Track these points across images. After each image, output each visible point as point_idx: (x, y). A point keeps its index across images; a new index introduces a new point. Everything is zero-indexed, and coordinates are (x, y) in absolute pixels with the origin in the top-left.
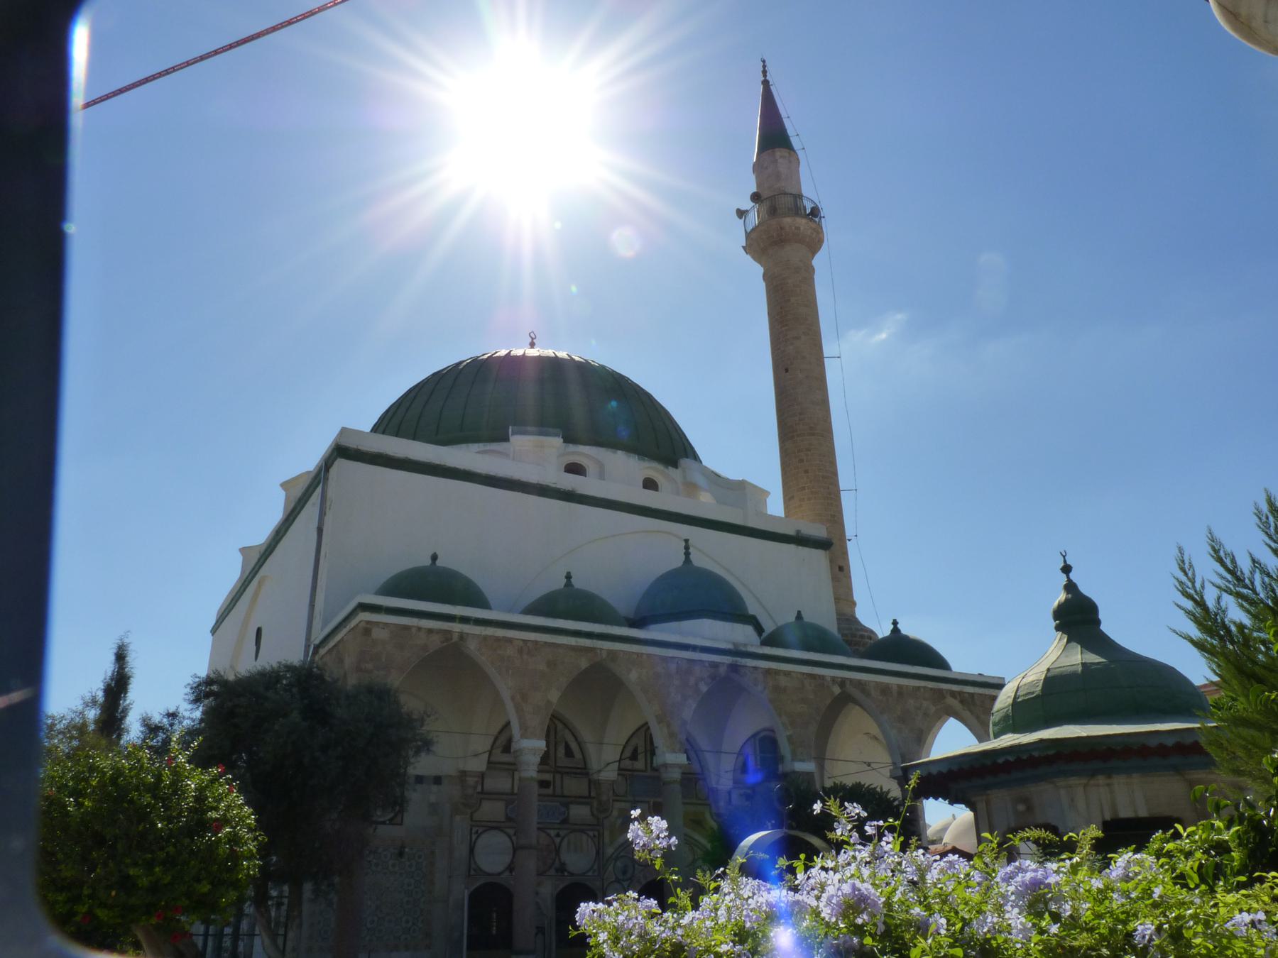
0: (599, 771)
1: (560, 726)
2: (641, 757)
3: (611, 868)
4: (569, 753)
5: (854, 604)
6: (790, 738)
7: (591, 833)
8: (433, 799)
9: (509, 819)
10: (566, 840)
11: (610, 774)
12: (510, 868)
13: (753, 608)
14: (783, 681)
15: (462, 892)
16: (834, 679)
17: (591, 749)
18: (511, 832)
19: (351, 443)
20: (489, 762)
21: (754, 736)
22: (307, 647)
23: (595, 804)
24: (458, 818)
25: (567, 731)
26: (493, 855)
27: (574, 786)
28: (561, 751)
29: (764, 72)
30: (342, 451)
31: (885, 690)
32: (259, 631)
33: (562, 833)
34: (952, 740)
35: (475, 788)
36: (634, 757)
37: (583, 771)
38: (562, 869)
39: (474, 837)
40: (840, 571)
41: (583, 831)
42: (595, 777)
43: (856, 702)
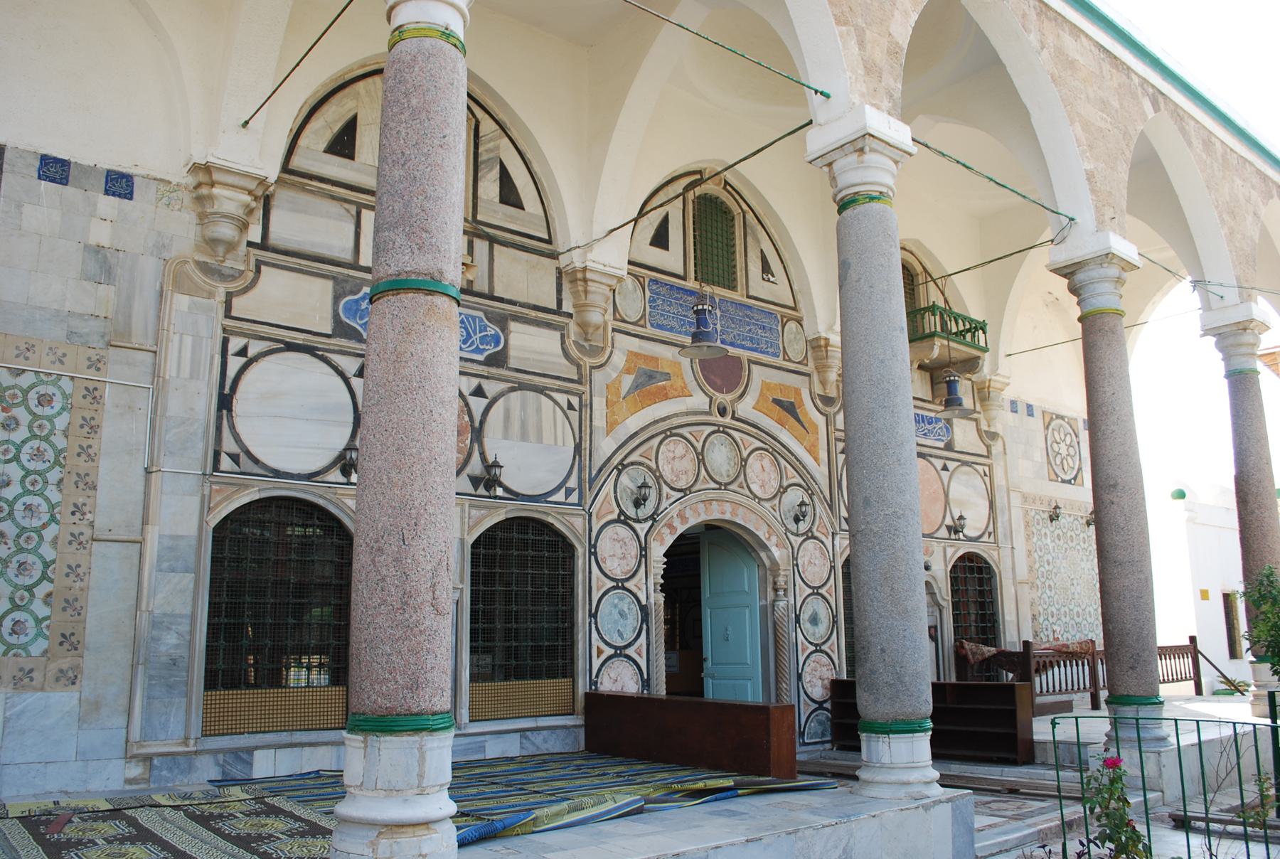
0: (589, 246)
3: (609, 486)
4: (509, 195)
6: (1090, 176)
7: (562, 399)
8: (100, 235)
9: (341, 329)
10: (500, 402)
12: (345, 464)
15: (184, 516)
16: (1144, 81)
18: (350, 365)
20: (285, 168)
23: (573, 327)
24: (182, 302)
25: (506, 139)
26: (293, 425)
27: (521, 278)
28: (490, 188)
31: (1208, 140)
33: (491, 388)
35: (244, 227)
36: (660, 239)
37: (543, 246)
38: (488, 480)
39: (234, 364)
41: (541, 390)
42: (576, 260)
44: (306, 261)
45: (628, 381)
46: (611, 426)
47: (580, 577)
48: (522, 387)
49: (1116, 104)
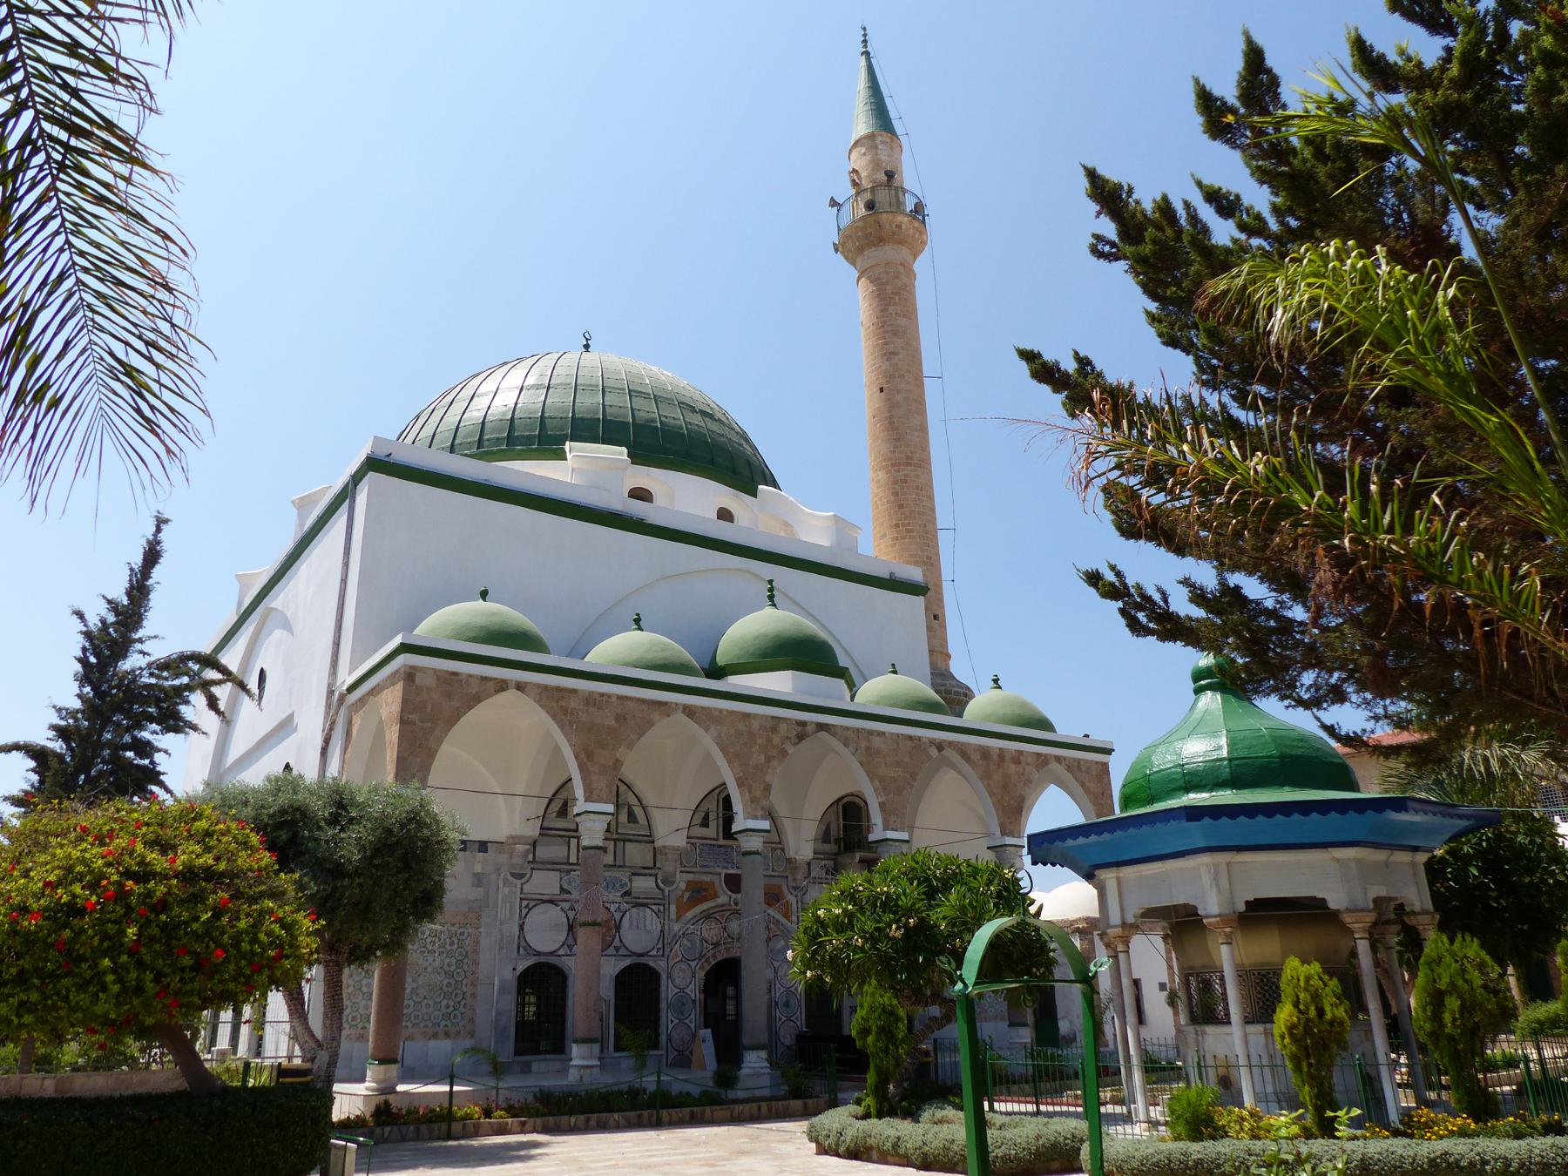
1: (623, 788)
2: (713, 824)
4: (632, 817)
5: (949, 657)
6: (882, 805)
8: (478, 868)
9: (563, 890)
11: (680, 841)
13: (843, 661)
14: (877, 742)
16: (932, 742)
17: (656, 815)
19: (381, 453)
21: (838, 801)
22: (331, 693)
26: (546, 932)
29: (865, 41)
30: (374, 464)
31: (985, 753)
32: (262, 671)
34: (1054, 809)
36: (705, 823)
37: (649, 839)
40: (936, 618)
41: (645, 905)
43: (956, 769)
44: (551, 865)
45: (687, 895)
46: (678, 919)
47: (663, 988)
48: (638, 905)
49: (907, 759)
